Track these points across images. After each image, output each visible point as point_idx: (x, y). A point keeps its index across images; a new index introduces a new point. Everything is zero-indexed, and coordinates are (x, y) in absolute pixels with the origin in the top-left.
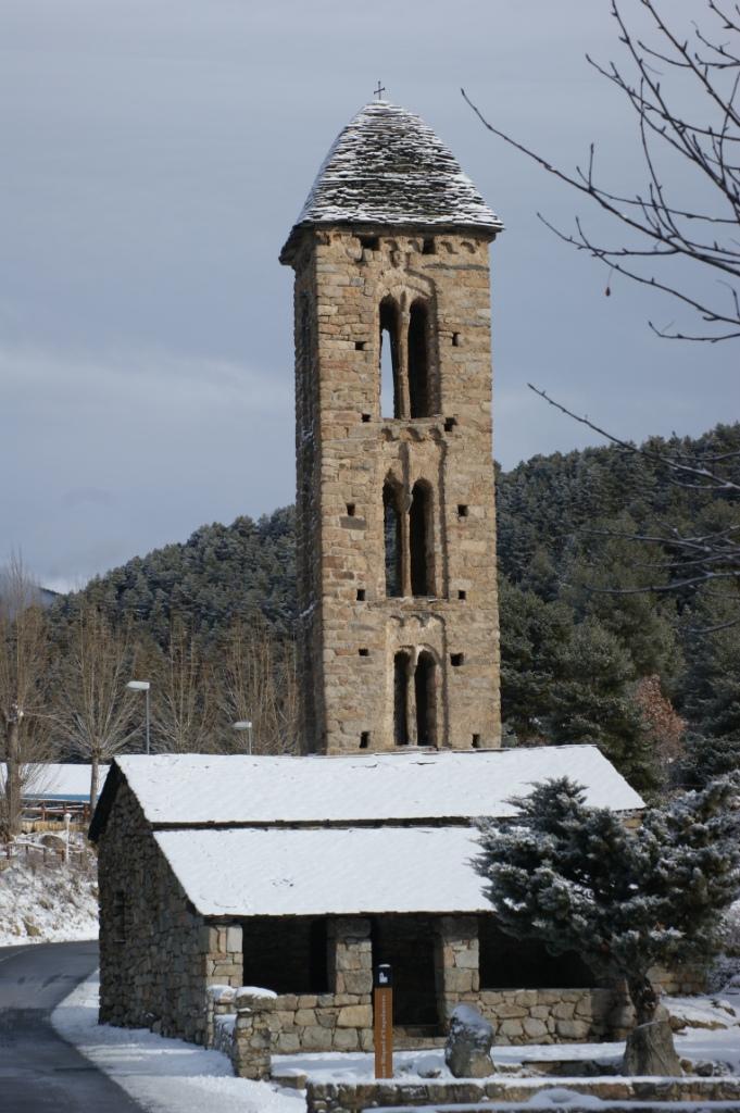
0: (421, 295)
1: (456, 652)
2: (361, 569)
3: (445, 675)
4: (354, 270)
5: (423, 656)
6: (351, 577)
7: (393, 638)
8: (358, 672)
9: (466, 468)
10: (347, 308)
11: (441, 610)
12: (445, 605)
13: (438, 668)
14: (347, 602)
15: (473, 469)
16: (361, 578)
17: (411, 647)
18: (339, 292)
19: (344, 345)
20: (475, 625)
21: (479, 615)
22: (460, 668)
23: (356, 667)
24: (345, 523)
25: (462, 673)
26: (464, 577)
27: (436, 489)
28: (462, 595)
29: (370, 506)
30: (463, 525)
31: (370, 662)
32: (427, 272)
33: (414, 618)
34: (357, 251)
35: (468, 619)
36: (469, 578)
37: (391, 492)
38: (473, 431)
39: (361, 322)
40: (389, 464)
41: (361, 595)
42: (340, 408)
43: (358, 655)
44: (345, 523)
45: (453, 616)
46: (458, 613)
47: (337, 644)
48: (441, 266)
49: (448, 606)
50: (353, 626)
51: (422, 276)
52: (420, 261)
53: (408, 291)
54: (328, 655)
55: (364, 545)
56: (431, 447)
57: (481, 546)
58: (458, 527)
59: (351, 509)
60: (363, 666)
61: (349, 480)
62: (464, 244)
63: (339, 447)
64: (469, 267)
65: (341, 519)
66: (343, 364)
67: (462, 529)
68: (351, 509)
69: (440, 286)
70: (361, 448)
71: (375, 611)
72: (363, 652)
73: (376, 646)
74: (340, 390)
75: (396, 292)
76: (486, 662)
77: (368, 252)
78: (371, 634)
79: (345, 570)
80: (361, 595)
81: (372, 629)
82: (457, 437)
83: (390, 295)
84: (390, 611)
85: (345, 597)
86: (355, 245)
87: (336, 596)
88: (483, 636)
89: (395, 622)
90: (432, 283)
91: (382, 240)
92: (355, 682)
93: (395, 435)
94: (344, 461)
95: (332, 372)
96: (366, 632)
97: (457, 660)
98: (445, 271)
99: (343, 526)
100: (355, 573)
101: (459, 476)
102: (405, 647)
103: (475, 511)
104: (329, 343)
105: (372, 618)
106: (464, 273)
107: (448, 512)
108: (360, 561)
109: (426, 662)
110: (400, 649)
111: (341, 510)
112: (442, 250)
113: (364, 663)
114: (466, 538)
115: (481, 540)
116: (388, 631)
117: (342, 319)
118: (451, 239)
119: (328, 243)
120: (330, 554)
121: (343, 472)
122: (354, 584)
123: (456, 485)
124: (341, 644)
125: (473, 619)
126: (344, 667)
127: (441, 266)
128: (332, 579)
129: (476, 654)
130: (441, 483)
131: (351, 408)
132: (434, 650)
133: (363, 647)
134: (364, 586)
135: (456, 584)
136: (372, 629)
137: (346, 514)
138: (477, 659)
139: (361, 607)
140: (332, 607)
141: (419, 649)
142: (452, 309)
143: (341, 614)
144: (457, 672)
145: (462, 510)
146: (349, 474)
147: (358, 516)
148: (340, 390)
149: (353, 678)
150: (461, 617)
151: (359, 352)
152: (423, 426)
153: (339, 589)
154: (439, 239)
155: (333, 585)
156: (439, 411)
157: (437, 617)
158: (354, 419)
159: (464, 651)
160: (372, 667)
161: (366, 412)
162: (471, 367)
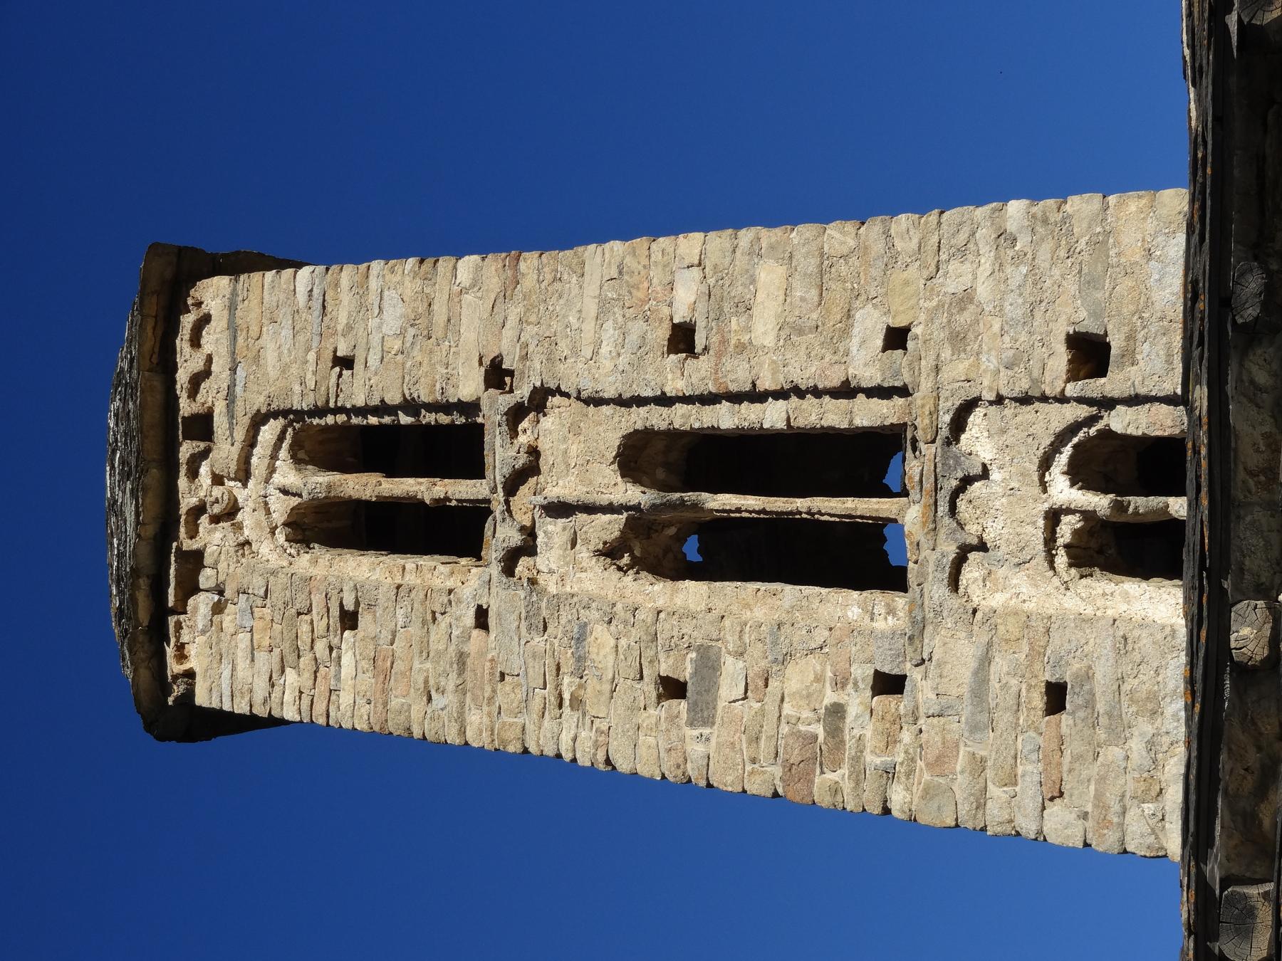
0: (284, 453)
1: (1060, 359)
2: (819, 679)
3: (1135, 400)
4: (228, 619)
5: (1079, 474)
6: (837, 711)
7: (1020, 581)
8: (1119, 731)
9: (589, 326)
10: (286, 646)
11: (935, 412)
12: (922, 396)
13: (1121, 421)
14: (906, 736)
15: (591, 308)
16: (840, 683)
17: (1053, 517)
18: (261, 656)
19: (347, 659)
20: (983, 291)
21: (952, 284)
22: (1116, 343)
23: (1101, 734)
24: (703, 716)
25: (1131, 337)
26: (846, 333)
27: (639, 418)
28: (896, 338)
29: (667, 627)
30: (715, 339)
31: (1088, 676)
32: (240, 434)
33: (962, 504)
34: (201, 604)
35: (965, 318)
36: (849, 315)
37: (651, 547)
38: (514, 312)
39: (309, 611)
40: (583, 554)
41: (889, 684)
42: (461, 689)
43: (1065, 718)
44: (703, 716)
45: (956, 369)
46: (946, 353)
47: (1029, 793)
48: (230, 398)
49: (926, 385)
50: (975, 728)
51: (251, 443)
52: (225, 451)
53: (287, 481)
54: (1062, 826)
55: (757, 660)
56: (549, 429)
57: (770, 275)
58: (719, 355)
59: (672, 688)
60: (1101, 707)
61: (607, 687)
62: (196, 342)
63: (536, 704)
64: (233, 329)
65: (691, 723)
66: (382, 667)
67: (724, 342)
68: (672, 688)
69: (258, 402)
70: (538, 641)
71: (933, 643)
72: (1056, 697)
73: (1036, 653)
74: (426, 682)
75: (281, 507)
76: (1099, 244)
77: (203, 583)
78: (1000, 665)
79: (819, 730)
80: (889, 684)
81: (985, 661)
82: (525, 357)
83: (285, 524)
84: (937, 590)
85: (890, 741)
86: (196, 609)
87: (889, 773)
88: (1018, 259)
89: (971, 573)
90: (259, 420)
91: (189, 545)
92: (1151, 745)
93: (516, 539)
94: (567, 696)
95: (395, 703)
96: (994, 685)
97: (1090, 353)
98: (239, 389)
99: (709, 721)
100: (830, 697)
101: (605, 350)
102: (1050, 541)
103: (685, 301)
104: (345, 699)
105: (955, 651)
106: (240, 340)
107: (643, 411)
108: (796, 678)
109: (1101, 460)
110: (1061, 559)
111: (673, 718)
112: (211, 394)
113: (1090, 704)
114: (748, 329)
115: (753, 281)
116: (997, 600)
117: (306, 660)
118: (182, 377)
119: (190, 674)
120: (777, 771)
121: (588, 695)
122: (857, 701)
123: (623, 361)
124: (1029, 770)
125: (965, 298)
126: (1102, 779)
127: (230, 398)
128: (840, 776)
129: (1071, 286)
130: (621, 402)
131: (462, 659)
132: (1061, 439)
133: (1039, 701)
134: (863, 673)
135: (866, 363)
136: (985, 661)
137: (683, 705)
138: (1089, 283)
139: (922, 688)
140: (917, 791)
141: (1062, 490)
142: (294, 370)
143: (939, 763)
144: (1130, 356)
145: (682, 339)
146: (592, 684)
147: (686, 672)
148: (426, 682)
149: (1136, 746)
150: (958, 340)
151: (364, 620)
152: (502, 454)
153: (873, 760)
154: (186, 407)
155: (859, 775)
156: (471, 408)
157: (959, 424)
158: (482, 654)
159: (1061, 329)
160: (1103, 673)
161: (469, 618)
162: (393, 318)
